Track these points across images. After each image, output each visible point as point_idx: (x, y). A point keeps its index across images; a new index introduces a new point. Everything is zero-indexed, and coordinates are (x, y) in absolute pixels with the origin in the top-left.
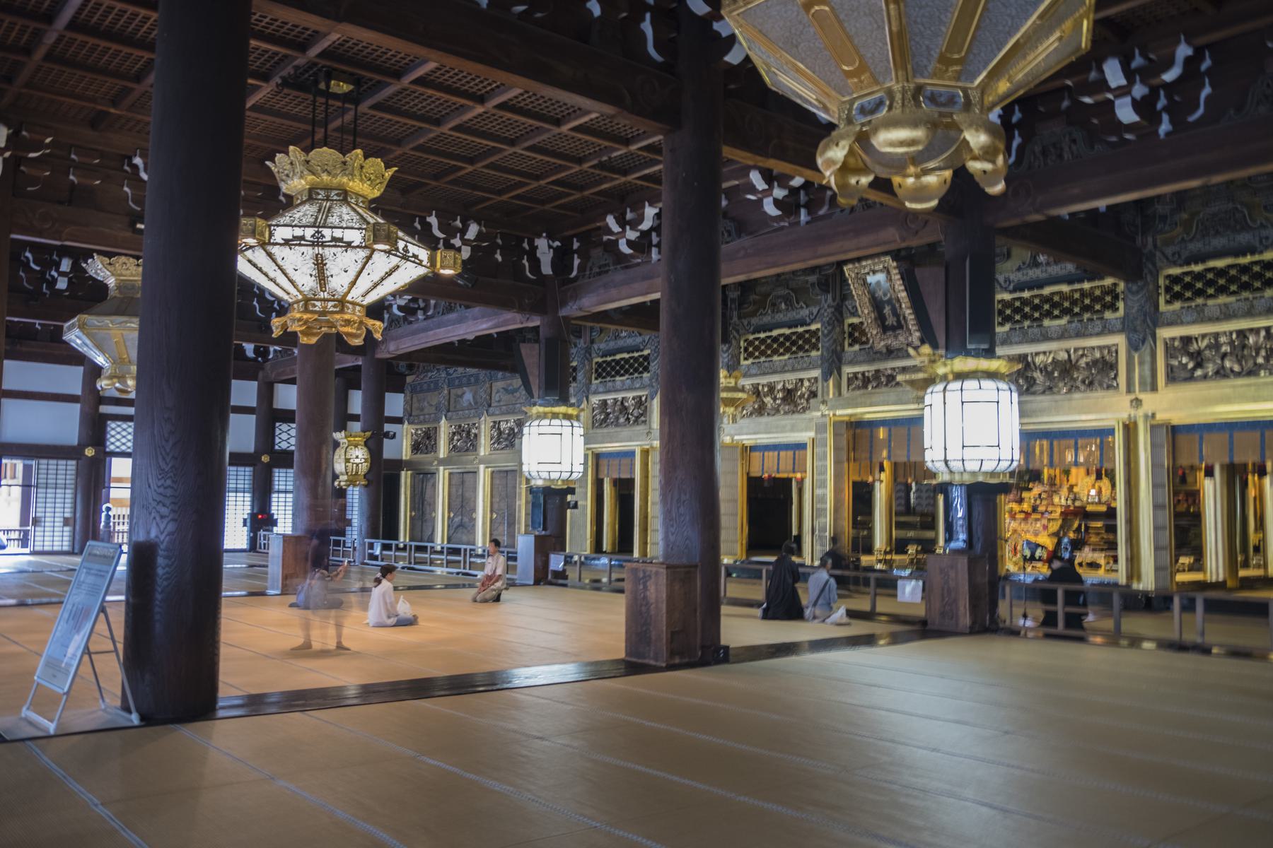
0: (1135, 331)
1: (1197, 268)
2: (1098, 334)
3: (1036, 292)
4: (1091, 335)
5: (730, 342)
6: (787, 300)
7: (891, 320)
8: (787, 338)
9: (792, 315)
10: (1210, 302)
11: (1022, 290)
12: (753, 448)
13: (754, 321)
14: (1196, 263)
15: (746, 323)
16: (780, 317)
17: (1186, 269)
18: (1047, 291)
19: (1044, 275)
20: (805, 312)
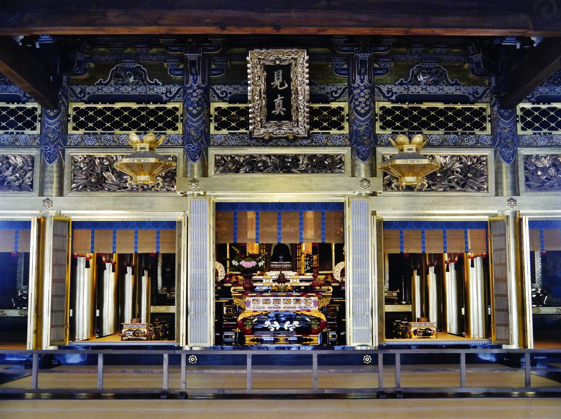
0: (507, 147)
1: (544, 106)
2: (472, 147)
3: (415, 105)
4: (467, 147)
5: (59, 108)
6: (136, 73)
7: (279, 110)
8: (134, 112)
9: (141, 90)
10: (554, 132)
11: (404, 102)
12: (77, 225)
13: (91, 90)
14: (544, 104)
15: (78, 90)
16: (126, 90)
17: (536, 106)
18: (425, 106)
19: (423, 92)
20: (161, 90)
